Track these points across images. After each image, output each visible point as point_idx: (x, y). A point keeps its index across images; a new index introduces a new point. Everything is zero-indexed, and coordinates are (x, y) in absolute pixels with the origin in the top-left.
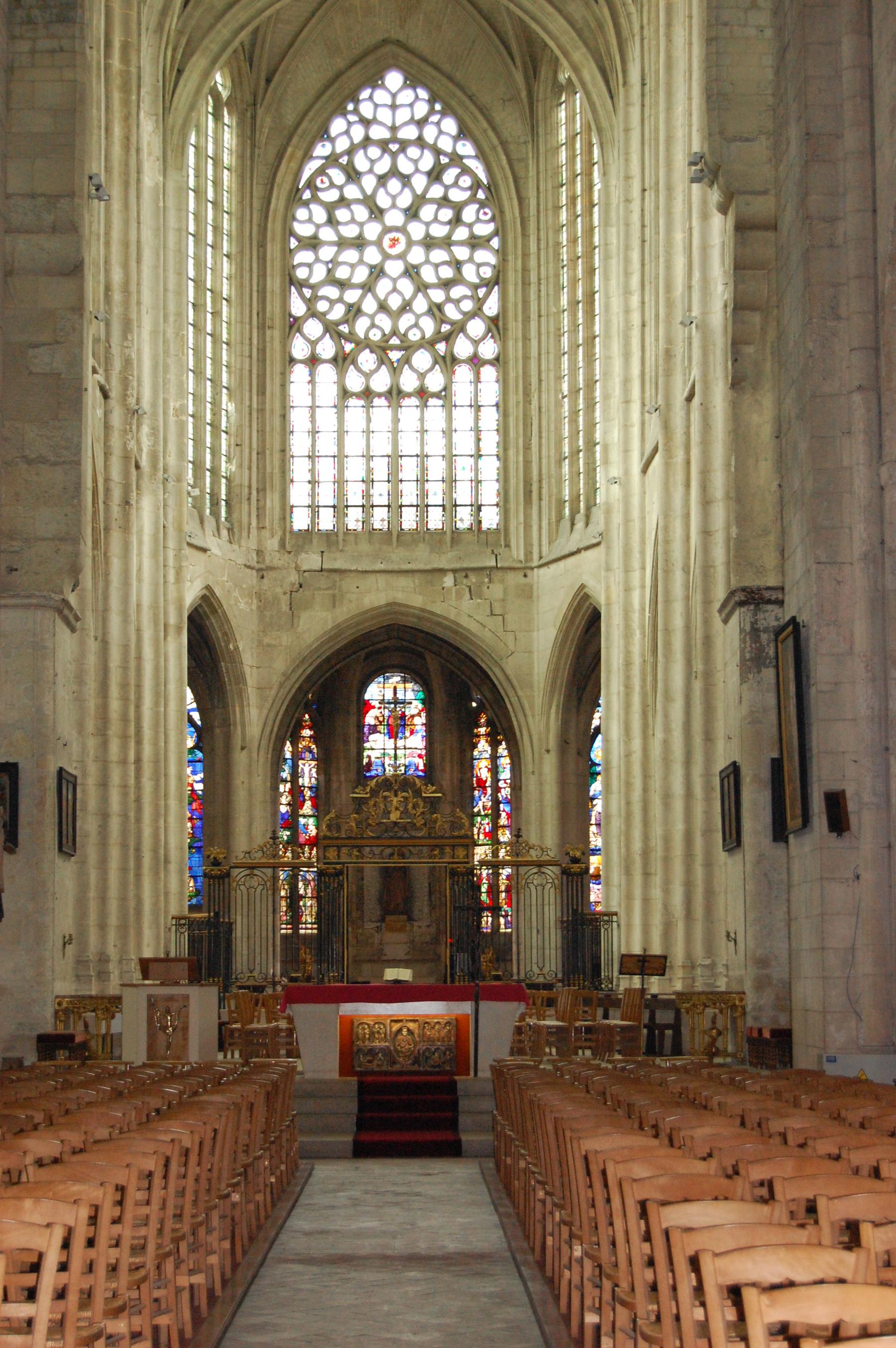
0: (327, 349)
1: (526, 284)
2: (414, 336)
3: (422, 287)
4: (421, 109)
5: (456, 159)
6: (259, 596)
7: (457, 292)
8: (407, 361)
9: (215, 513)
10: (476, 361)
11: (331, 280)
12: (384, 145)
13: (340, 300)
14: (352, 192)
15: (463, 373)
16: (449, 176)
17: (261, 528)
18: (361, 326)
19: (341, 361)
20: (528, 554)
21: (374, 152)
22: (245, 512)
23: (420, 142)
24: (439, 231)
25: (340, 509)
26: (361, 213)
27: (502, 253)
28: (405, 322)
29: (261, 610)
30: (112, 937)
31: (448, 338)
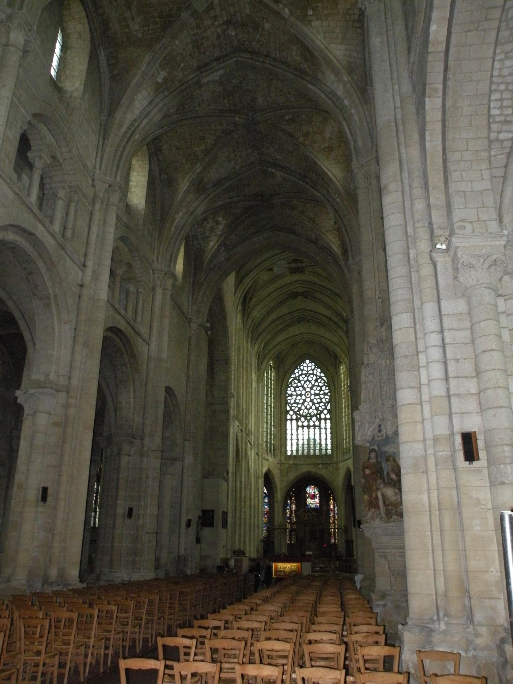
0: (294, 417)
3: (314, 404)
4: (313, 367)
5: (320, 377)
6: (280, 469)
7: (321, 404)
8: (311, 419)
9: (270, 452)
10: (325, 419)
11: (295, 403)
12: (305, 375)
13: (297, 407)
14: (299, 384)
15: (323, 422)
16: (319, 381)
17: (280, 455)
18: (301, 412)
19: (297, 420)
20: (337, 460)
21: (304, 376)
22: (277, 452)
23: (313, 374)
24: (317, 392)
25: (297, 450)
26: (301, 389)
28: (311, 411)
29: (281, 472)
30: (242, 545)
31: (320, 414)
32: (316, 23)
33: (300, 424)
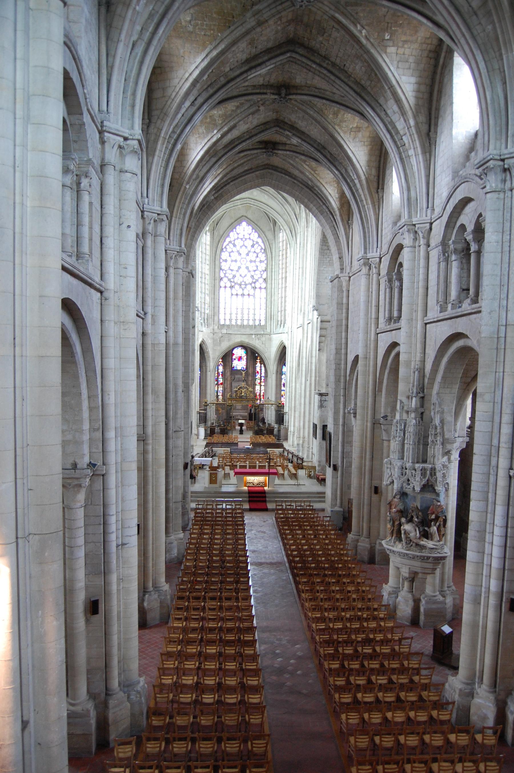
0: (228, 284)
1: (272, 272)
2: (247, 283)
5: (257, 243)
7: (257, 272)
10: (260, 288)
11: (229, 269)
12: (242, 239)
18: (236, 280)
19: (232, 287)
20: (271, 331)
21: (239, 240)
22: (210, 321)
25: (230, 320)
27: (267, 264)
31: (255, 283)
32: (391, 50)
33: (234, 292)
